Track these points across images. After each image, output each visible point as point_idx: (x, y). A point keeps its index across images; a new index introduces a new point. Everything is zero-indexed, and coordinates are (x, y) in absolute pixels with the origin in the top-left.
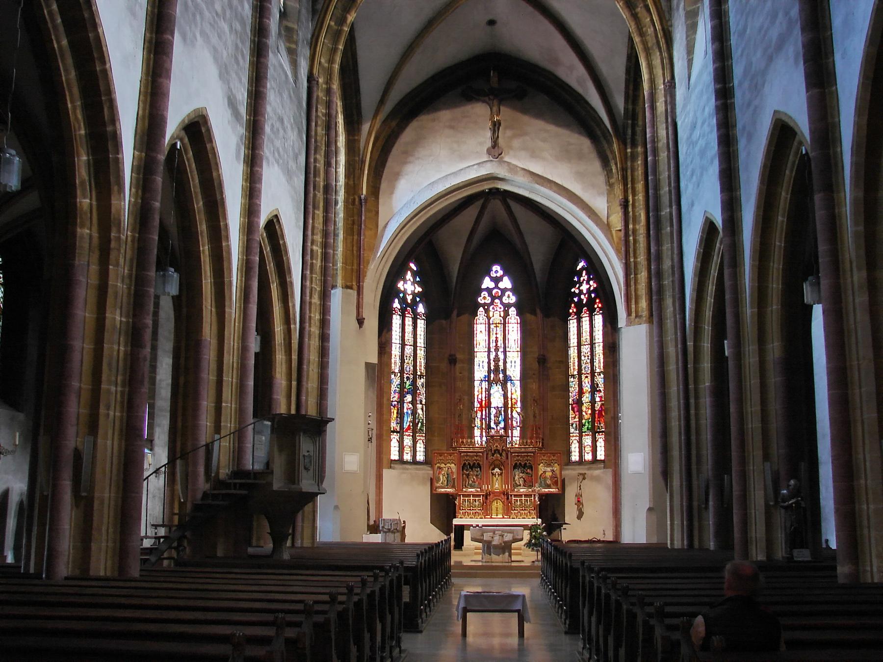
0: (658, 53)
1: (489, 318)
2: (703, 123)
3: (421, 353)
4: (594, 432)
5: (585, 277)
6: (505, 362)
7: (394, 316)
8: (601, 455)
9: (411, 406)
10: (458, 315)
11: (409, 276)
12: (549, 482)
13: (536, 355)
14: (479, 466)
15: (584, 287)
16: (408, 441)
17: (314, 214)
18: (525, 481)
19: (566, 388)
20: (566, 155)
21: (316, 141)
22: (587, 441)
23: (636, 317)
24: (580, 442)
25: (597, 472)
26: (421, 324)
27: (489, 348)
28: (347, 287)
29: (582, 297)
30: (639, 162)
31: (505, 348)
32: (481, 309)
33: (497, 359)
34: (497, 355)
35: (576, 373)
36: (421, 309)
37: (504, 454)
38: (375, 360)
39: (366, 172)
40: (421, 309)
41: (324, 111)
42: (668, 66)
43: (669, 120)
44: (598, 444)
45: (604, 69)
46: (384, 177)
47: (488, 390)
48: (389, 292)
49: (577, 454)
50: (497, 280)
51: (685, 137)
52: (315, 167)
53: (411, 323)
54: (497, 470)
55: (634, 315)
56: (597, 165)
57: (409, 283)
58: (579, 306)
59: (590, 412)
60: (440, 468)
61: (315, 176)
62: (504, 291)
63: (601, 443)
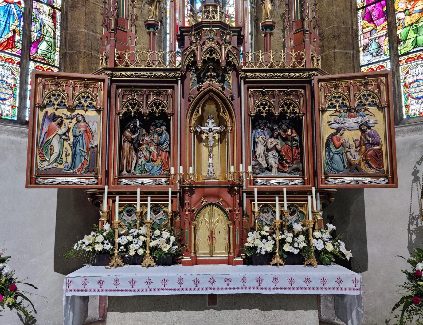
12: (355, 157)
14: (165, 119)
18: (281, 158)
37: (231, 78)
54: (210, 125)
60: (54, 118)
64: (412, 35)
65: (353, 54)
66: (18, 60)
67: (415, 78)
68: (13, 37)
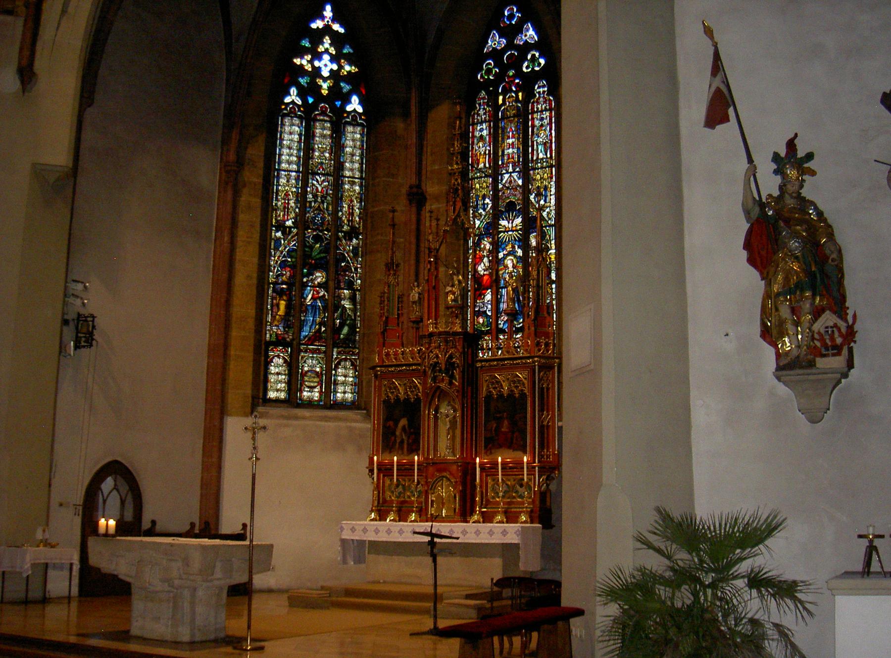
3: (353, 189)
16: (311, 363)
36: (355, 105)
40: (355, 105)
66: (323, 348)
68: (320, 329)
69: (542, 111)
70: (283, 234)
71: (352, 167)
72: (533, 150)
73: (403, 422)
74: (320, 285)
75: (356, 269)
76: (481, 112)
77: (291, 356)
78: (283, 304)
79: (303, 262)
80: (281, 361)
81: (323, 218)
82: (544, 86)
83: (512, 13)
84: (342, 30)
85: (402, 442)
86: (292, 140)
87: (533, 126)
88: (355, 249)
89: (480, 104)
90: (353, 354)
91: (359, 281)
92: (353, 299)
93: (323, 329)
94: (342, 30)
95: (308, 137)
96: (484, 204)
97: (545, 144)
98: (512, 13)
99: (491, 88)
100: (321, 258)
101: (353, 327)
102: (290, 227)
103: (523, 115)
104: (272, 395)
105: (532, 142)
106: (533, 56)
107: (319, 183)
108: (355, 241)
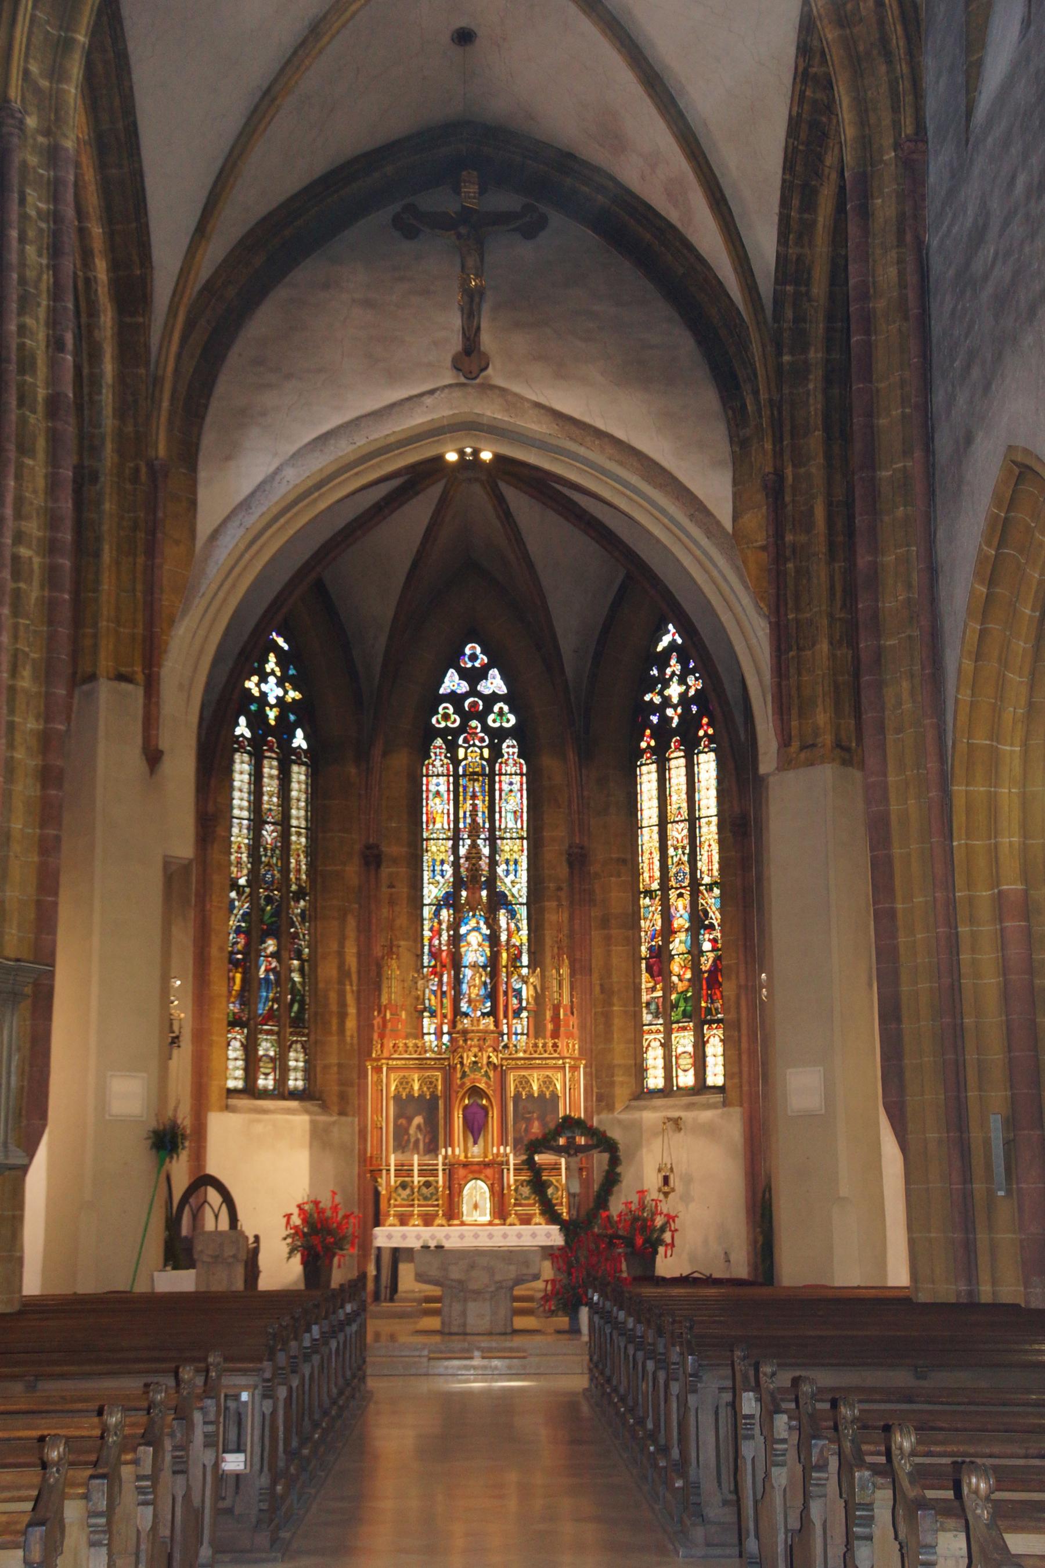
0: (883, 69)
1: (456, 762)
2: (1006, 223)
3: (299, 841)
4: (700, 1021)
5: (675, 666)
6: (493, 863)
7: (237, 756)
8: (715, 1076)
9: (274, 964)
10: (385, 754)
11: (271, 664)
13: (566, 846)
15: (674, 691)
16: (266, 1047)
17: (20, 466)
19: (634, 918)
20: (638, 371)
21: (22, 281)
22: (684, 1042)
23: (803, 748)
24: (666, 1045)
25: (706, 1116)
26: (299, 775)
27: (457, 830)
28: (121, 677)
29: (670, 712)
30: (811, 386)
31: (492, 829)
32: (439, 742)
33: (474, 853)
34: (474, 846)
35: (655, 886)
36: (299, 740)
38: (184, 849)
39: (165, 404)
40: (299, 740)
41: (42, 206)
42: (909, 98)
43: (909, 237)
44: (710, 1050)
45: (731, 161)
46: (208, 420)
47: (455, 926)
48: (226, 700)
49: (661, 1073)
50: (474, 677)
51: (951, 273)
52: (22, 347)
53: (275, 772)
55: (795, 745)
56: (709, 398)
57: (272, 680)
58: (663, 733)
59: (688, 975)
61: (22, 370)
62: (491, 699)
63: (715, 1048)
64: (682, 1004)
65: (635, 1012)
67: (684, 1050)
69: (511, 774)
70: (238, 893)
71: (298, 815)
72: (501, 817)
73: (418, 1120)
74: (273, 955)
75: (304, 935)
76: (438, 763)
77: (247, 1038)
78: (238, 976)
79: (256, 929)
80: (237, 1044)
81: (273, 876)
82: (513, 747)
83: (474, 653)
84: (286, 647)
85: (417, 1141)
86: (242, 781)
87: (501, 790)
88: (303, 914)
89: (435, 753)
90: (303, 1035)
91: (307, 950)
92: (301, 971)
93: (276, 1006)
94: (286, 647)
95: (257, 776)
96: (442, 871)
97: (515, 812)
98: (474, 653)
99: (451, 739)
100: (273, 923)
101: (302, 1003)
102: (244, 887)
103: (490, 776)
104: (231, 1084)
105: (500, 808)
106: (501, 709)
107: (269, 834)
108: (302, 903)
